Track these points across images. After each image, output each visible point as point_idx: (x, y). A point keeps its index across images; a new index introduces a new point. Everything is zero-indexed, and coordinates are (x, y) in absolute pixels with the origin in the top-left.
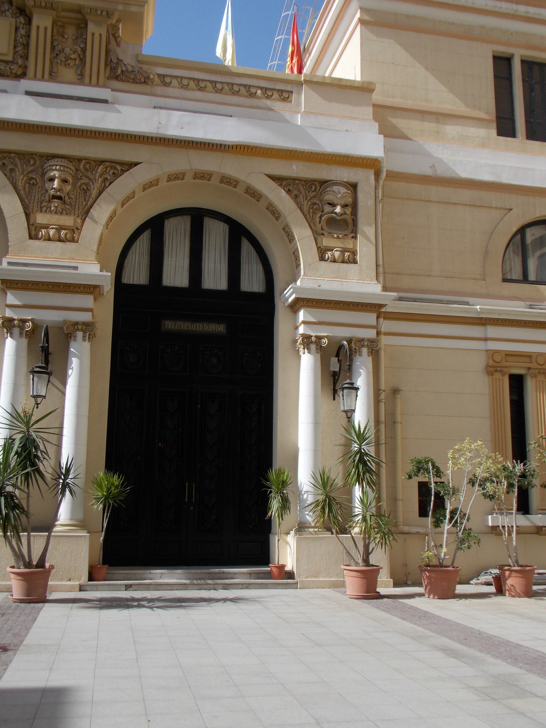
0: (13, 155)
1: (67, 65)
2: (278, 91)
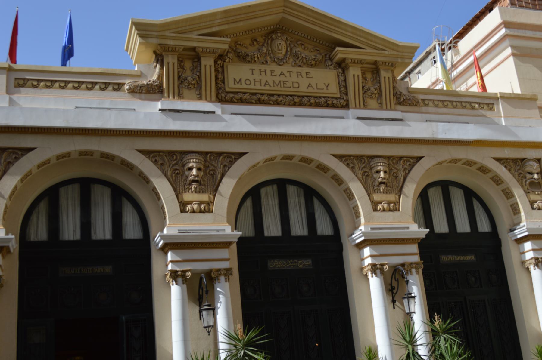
0: (352, 158)
1: (371, 98)
2: (486, 104)
